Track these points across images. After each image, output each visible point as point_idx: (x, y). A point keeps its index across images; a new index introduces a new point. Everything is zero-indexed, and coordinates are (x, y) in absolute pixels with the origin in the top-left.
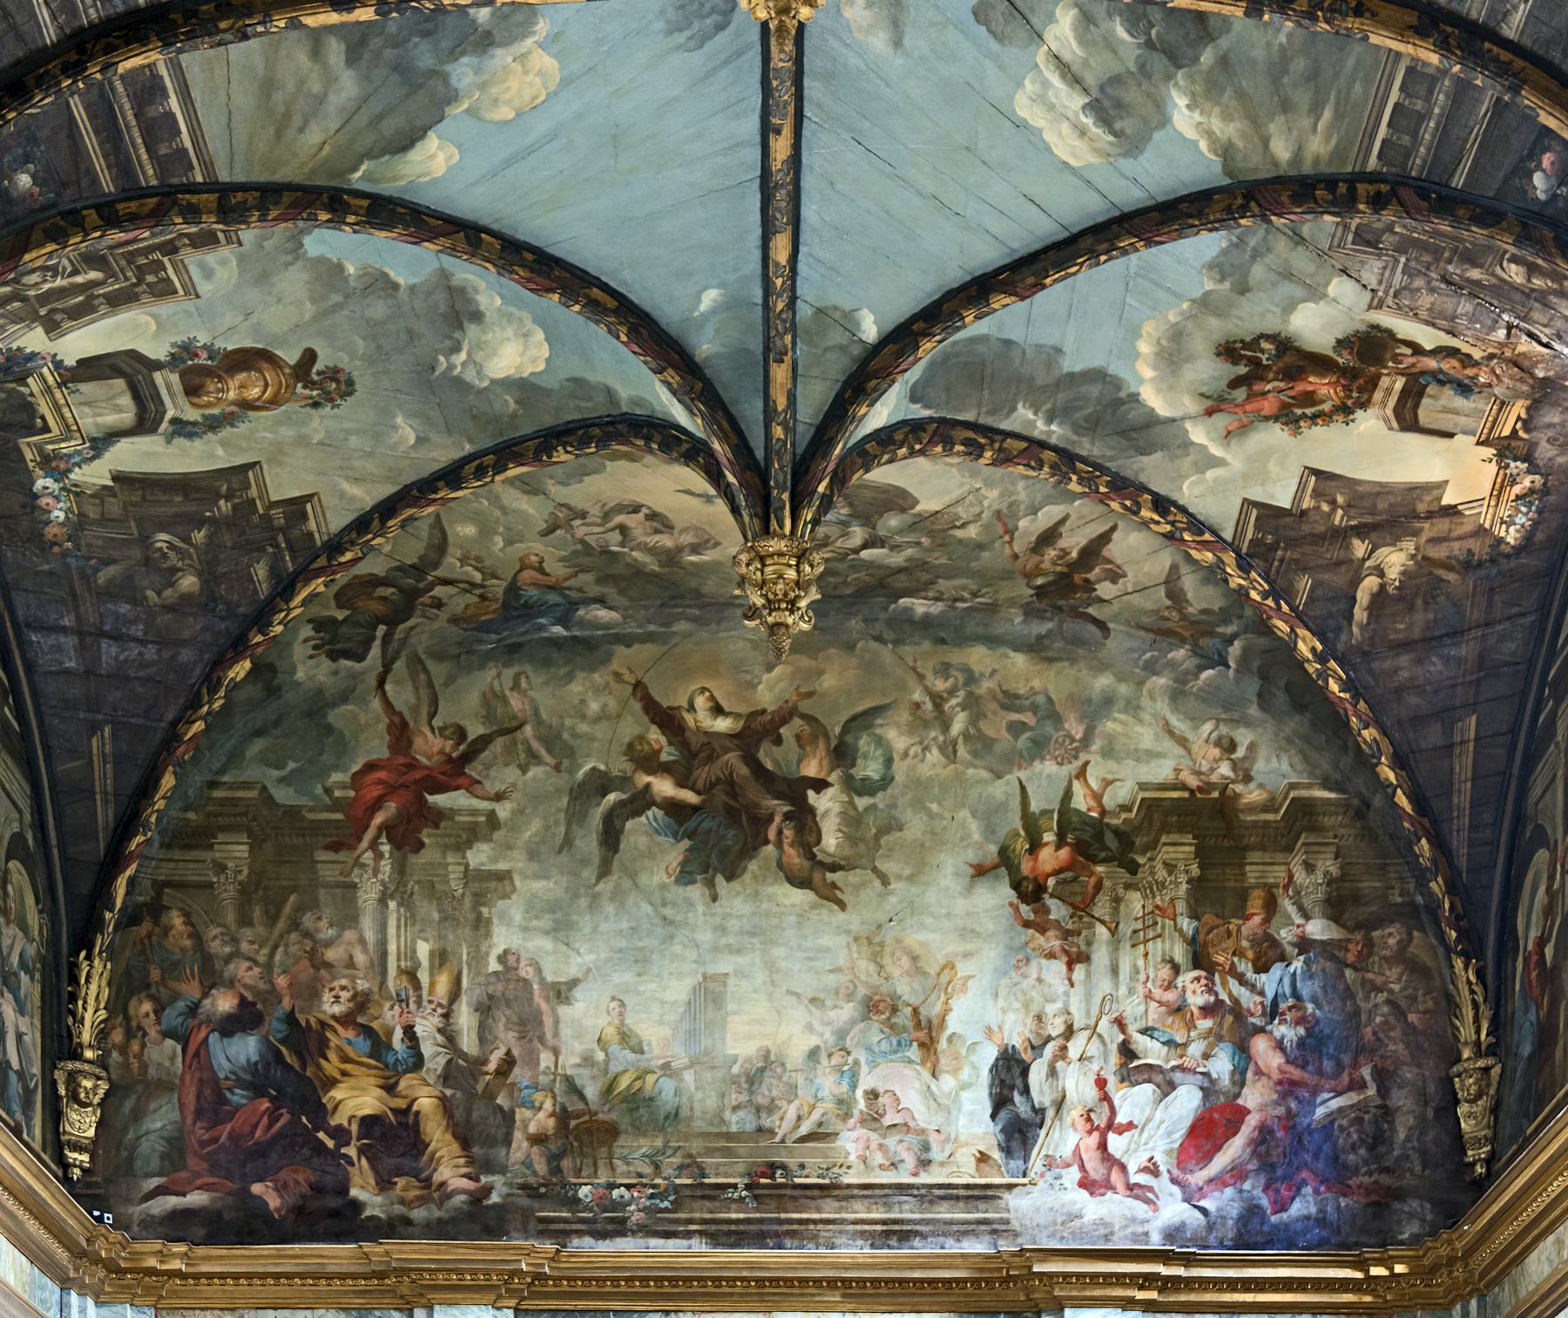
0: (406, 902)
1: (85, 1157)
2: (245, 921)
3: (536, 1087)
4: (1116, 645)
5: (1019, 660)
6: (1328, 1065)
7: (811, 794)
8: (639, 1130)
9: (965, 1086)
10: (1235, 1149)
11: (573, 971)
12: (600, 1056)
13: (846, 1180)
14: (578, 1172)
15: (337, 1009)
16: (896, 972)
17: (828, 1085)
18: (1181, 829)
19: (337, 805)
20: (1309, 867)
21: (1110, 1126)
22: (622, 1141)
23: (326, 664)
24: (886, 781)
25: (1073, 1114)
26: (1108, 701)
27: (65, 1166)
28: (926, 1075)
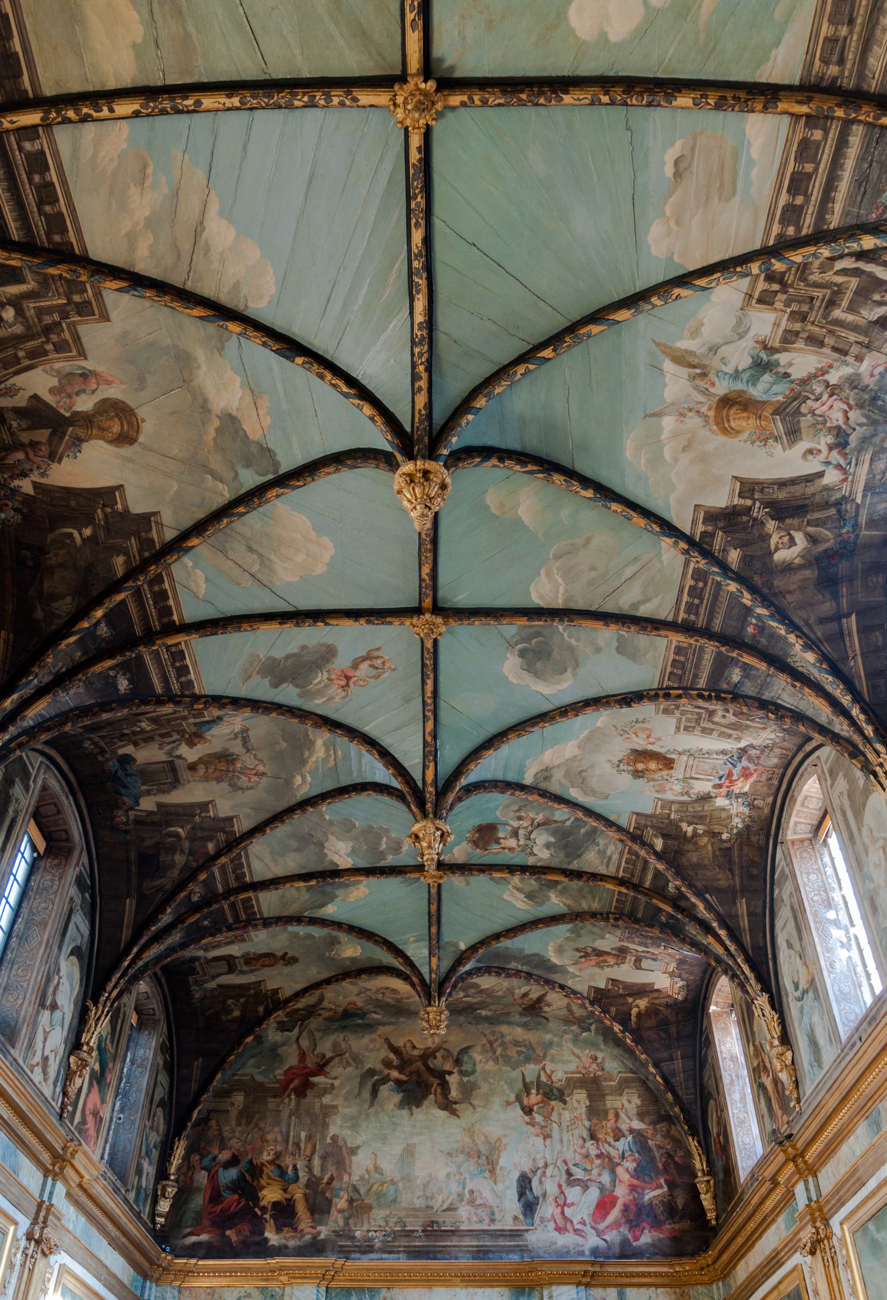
0: (299, 1117)
1: (162, 1220)
2: (239, 1124)
3: (341, 1189)
4: (552, 1025)
5: (519, 1030)
6: (647, 1178)
7: (447, 1077)
8: (380, 1206)
9: (507, 1188)
10: (615, 1213)
11: (358, 1142)
12: (367, 1176)
13: (462, 1228)
14: (356, 1225)
15: (269, 1158)
16: (479, 1142)
17: (455, 1188)
18: (581, 1087)
19: (277, 1081)
20: (629, 1101)
21: (565, 1204)
22: (373, 1212)
23: (279, 1033)
24: (474, 1072)
25: (550, 1199)
26: (551, 1043)
27: (154, 1222)
28: (492, 1183)
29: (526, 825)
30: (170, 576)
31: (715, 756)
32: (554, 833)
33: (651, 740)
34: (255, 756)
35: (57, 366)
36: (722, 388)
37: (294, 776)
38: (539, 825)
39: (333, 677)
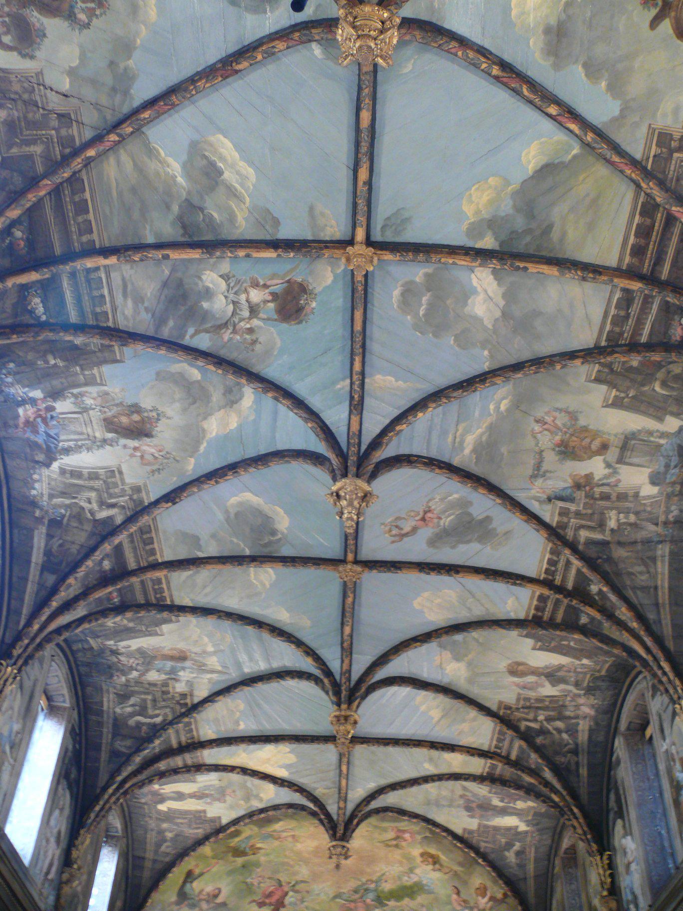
29: (242, 324)
30: (527, 615)
31: (72, 444)
32: (205, 316)
33: (138, 454)
34: (537, 445)
35: (534, 694)
36: (188, 664)
37: (508, 410)
38: (225, 325)
39: (436, 521)
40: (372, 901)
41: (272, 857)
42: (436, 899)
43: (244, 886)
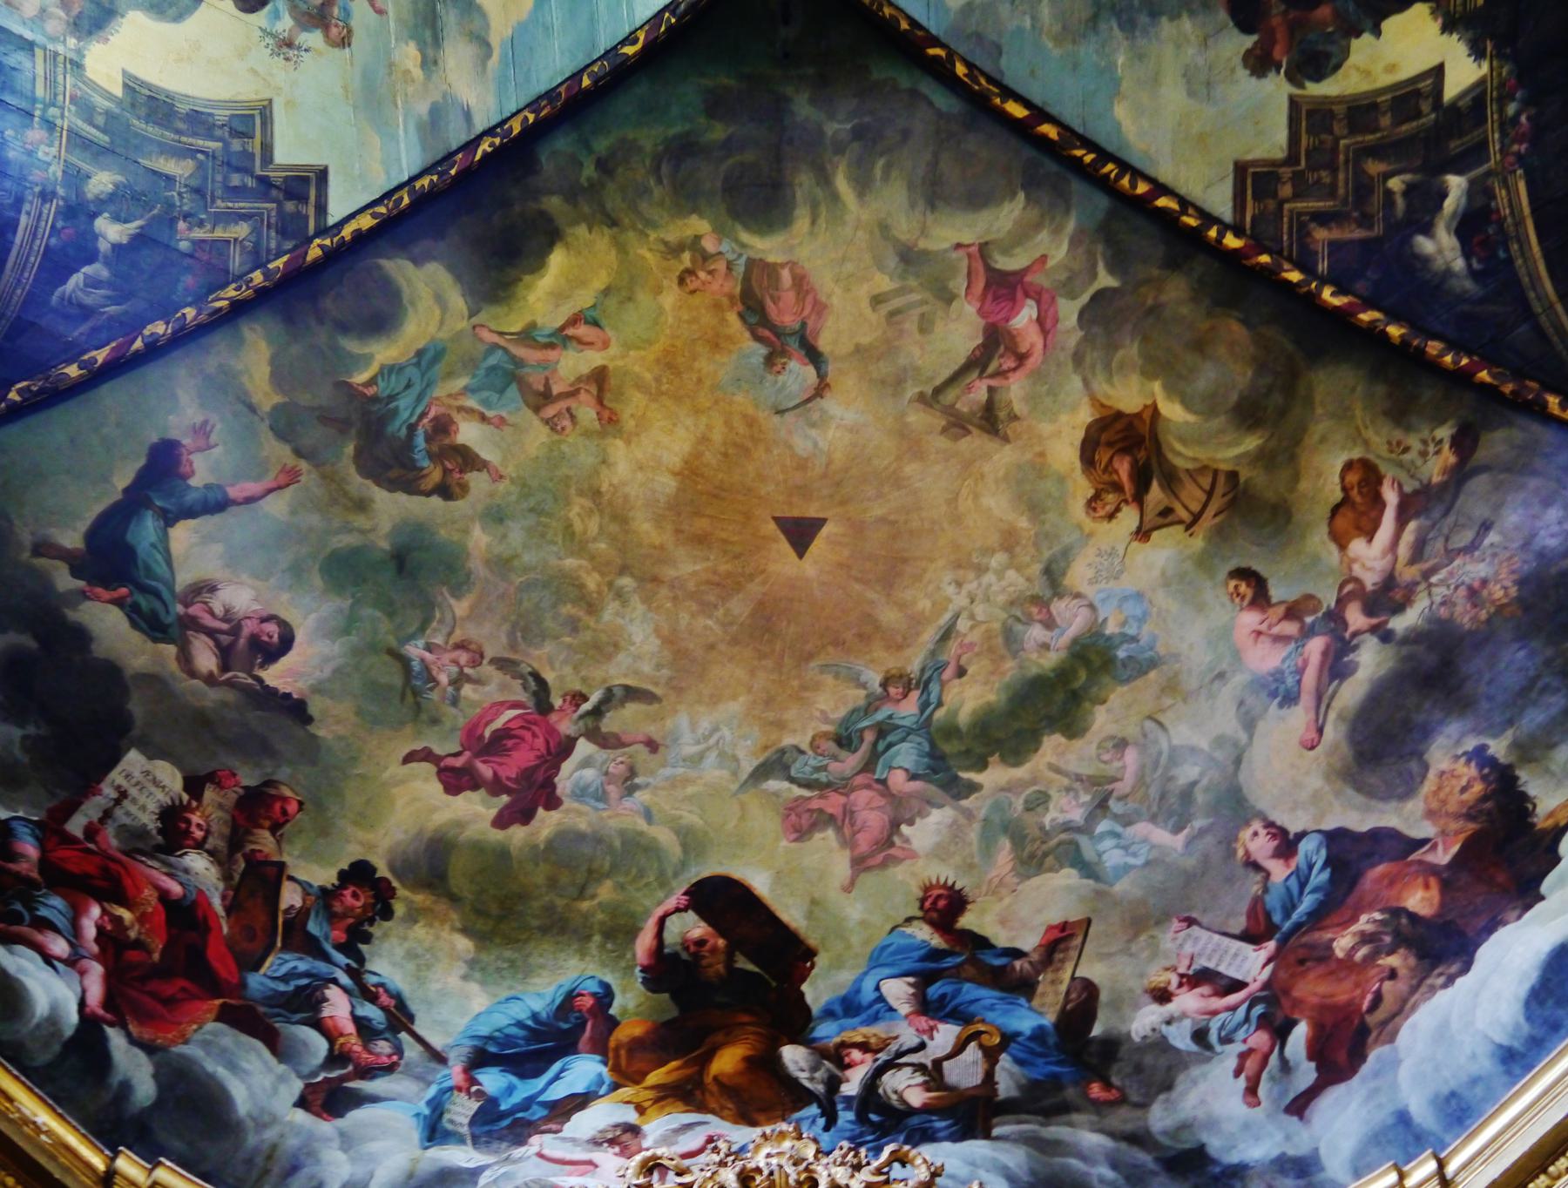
40: (913, 777)
41: (516, 534)
42: (1171, 687)
43: (391, 676)
